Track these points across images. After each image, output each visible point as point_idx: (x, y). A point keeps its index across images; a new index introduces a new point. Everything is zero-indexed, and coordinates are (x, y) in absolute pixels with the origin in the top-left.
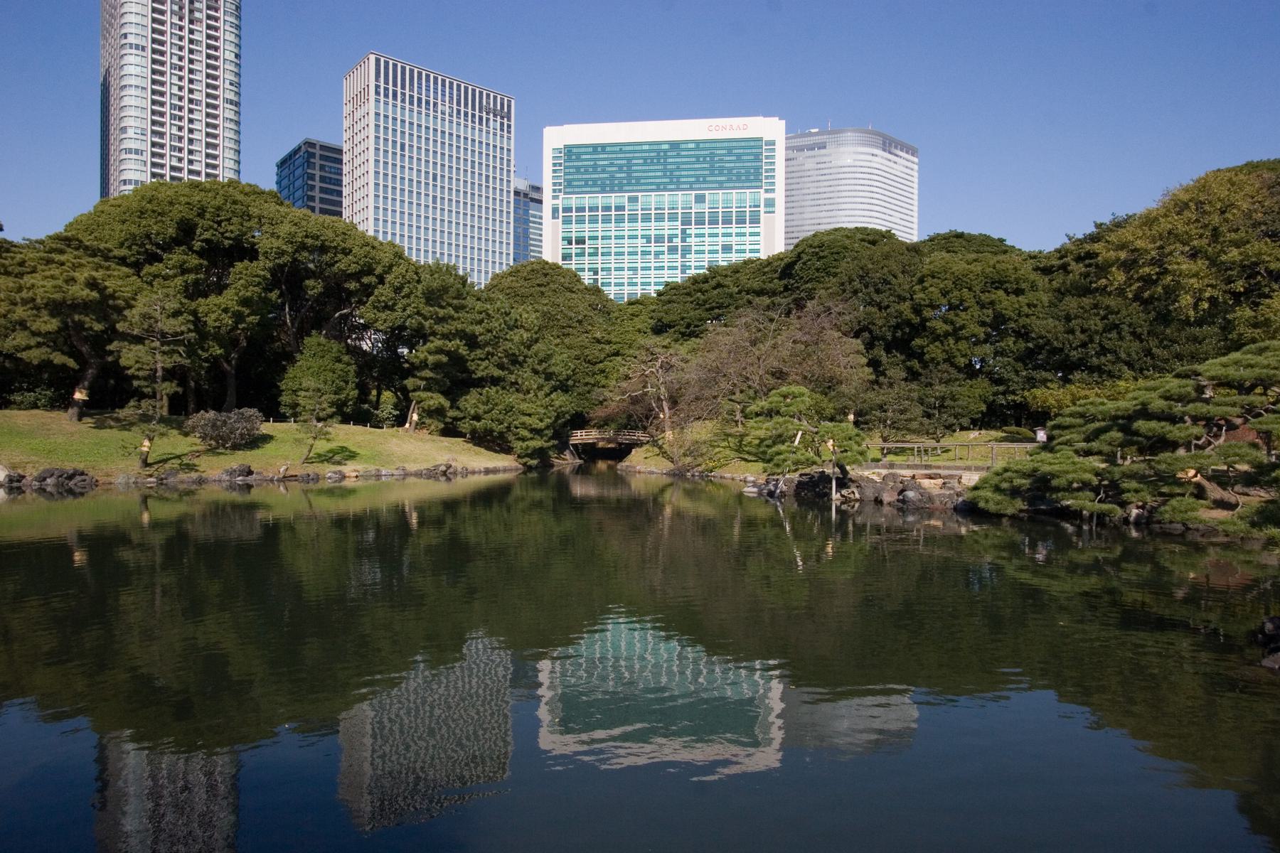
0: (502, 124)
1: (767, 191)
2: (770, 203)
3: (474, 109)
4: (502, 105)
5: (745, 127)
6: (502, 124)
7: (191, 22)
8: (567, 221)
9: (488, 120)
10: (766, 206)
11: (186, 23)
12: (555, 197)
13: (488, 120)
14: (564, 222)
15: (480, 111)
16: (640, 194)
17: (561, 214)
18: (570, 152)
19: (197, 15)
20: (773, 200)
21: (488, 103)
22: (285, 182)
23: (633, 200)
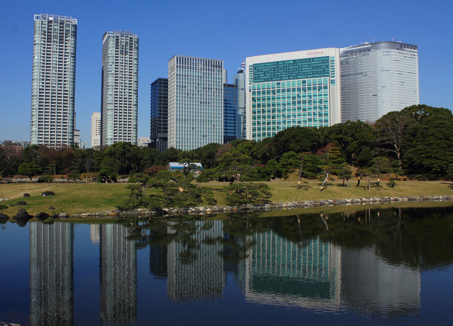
0: (219, 70)
2: (333, 82)
3: (209, 67)
4: (219, 63)
5: (322, 52)
6: (219, 70)
7: (125, 55)
8: (254, 93)
9: (214, 69)
11: (124, 56)
13: (214, 69)
15: (211, 67)
17: (252, 91)
18: (255, 67)
20: (334, 80)
21: (214, 64)
22: (153, 87)
23: (278, 84)
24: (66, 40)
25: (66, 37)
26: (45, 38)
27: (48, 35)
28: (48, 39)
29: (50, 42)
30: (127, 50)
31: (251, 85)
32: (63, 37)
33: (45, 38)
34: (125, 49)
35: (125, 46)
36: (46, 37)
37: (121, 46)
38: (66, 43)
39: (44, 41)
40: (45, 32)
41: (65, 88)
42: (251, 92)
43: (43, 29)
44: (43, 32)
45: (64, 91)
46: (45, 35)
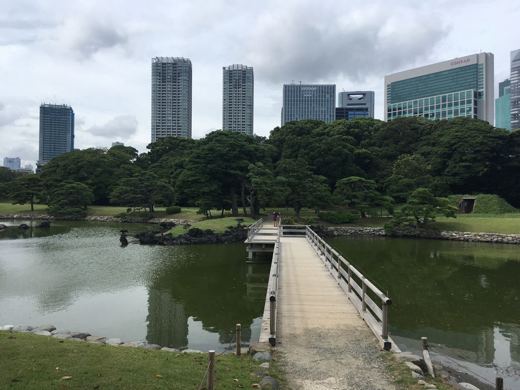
20: (483, 92)
23: (415, 103)
24: (178, 80)
26: (160, 79)
28: (163, 79)
29: (165, 82)
30: (240, 83)
33: (160, 79)
39: (160, 82)
40: (160, 73)
41: (178, 123)
43: (158, 71)
44: (158, 74)
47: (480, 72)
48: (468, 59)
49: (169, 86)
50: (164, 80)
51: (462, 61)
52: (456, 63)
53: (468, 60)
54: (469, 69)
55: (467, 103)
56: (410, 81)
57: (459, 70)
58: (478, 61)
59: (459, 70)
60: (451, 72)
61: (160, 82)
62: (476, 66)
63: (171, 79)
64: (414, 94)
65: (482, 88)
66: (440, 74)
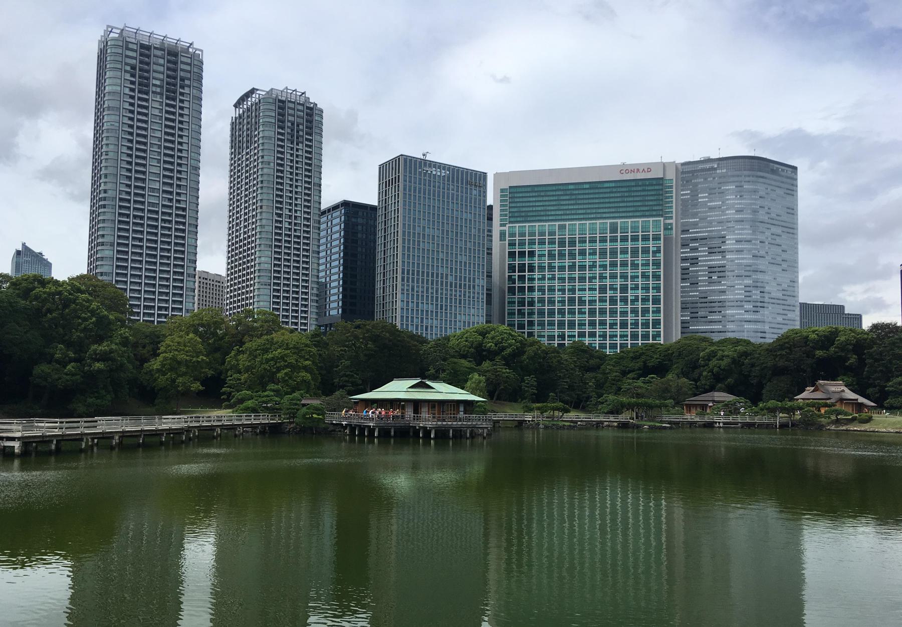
0: (480, 191)
1: (666, 218)
7: (297, 144)
8: (512, 244)
10: (665, 229)
12: (501, 225)
14: (509, 245)
16: (567, 223)
17: (507, 238)
19: (300, 139)
20: (671, 224)
23: (562, 227)
24: (182, 94)
25: (182, 87)
27: (140, 77)
31: (506, 228)
32: (175, 85)
33: (132, 83)
34: (298, 132)
35: (298, 126)
36: (137, 80)
37: (289, 124)
38: (182, 101)
40: (133, 67)
41: (178, 201)
42: (507, 242)
44: (128, 68)
45: (177, 208)
46: (133, 76)
47: (667, 192)
48: (648, 168)
49: (156, 105)
50: (144, 86)
51: (638, 170)
52: (627, 172)
53: (649, 170)
54: (652, 185)
55: (622, 240)
56: (544, 189)
57: (633, 184)
58: (664, 174)
59: (633, 184)
60: (619, 184)
61: (132, 90)
62: (659, 181)
63: (161, 87)
64: (553, 213)
65: (671, 218)
66: (599, 186)
